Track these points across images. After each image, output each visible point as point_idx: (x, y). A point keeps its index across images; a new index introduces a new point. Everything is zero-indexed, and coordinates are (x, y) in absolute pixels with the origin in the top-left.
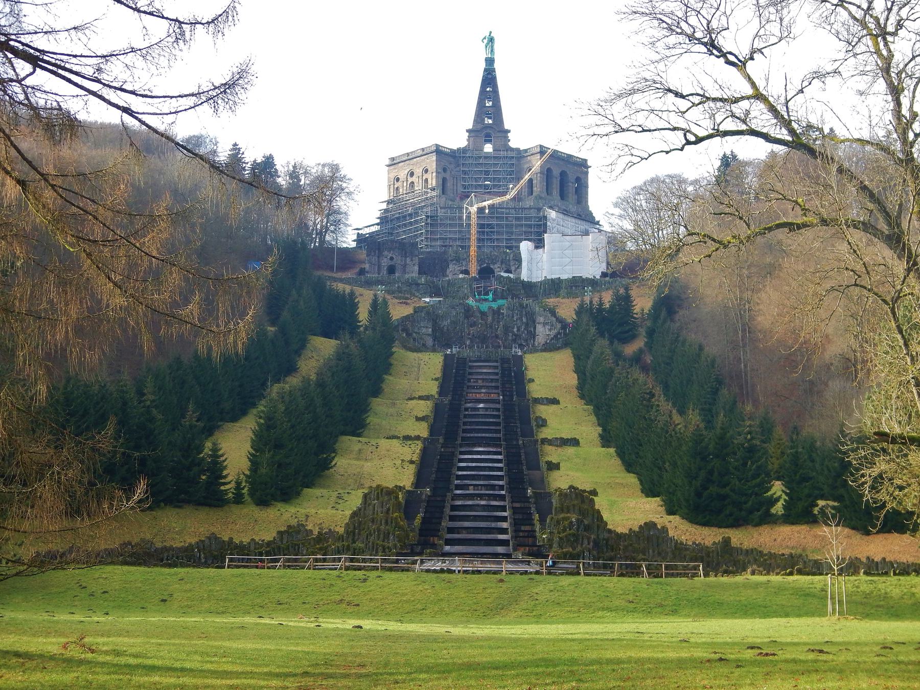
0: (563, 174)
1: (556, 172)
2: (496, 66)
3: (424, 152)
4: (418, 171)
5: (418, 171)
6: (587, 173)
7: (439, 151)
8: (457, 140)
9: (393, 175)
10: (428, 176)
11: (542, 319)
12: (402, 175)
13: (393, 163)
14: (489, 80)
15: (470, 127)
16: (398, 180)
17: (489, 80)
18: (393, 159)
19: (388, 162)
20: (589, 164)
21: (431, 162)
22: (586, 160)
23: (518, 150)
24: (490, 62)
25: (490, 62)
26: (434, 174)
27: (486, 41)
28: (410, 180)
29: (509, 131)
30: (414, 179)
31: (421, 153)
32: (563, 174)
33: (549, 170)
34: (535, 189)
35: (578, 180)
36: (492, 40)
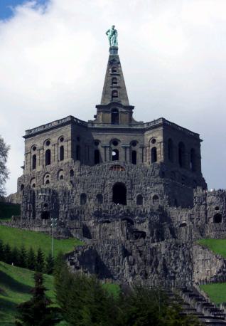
0: (181, 145)
1: (176, 143)
2: (120, 53)
3: (61, 124)
4: (54, 140)
5: (54, 140)
6: (199, 146)
7: (73, 121)
8: (87, 114)
9: (31, 144)
10: (64, 144)
11: (201, 257)
12: (39, 144)
13: (30, 135)
14: (114, 63)
15: (99, 103)
16: (35, 149)
17: (114, 63)
18: (30, 131)
19: (24, 134)
20: (201, 138)
21: (67, 131)
22: (198, 135)
23: (141, 123)
24: (114, 50)
25: (114, 50)
26: (70, 142)
27: (110, 34)
28: (46, 148)
29: (133, 108)
30: (50, 147)
31: (57, 124)
32: (181, 145)
33: (170, 140)
34: (158, 156)
35: (192, 150)
36: (114, 32)
